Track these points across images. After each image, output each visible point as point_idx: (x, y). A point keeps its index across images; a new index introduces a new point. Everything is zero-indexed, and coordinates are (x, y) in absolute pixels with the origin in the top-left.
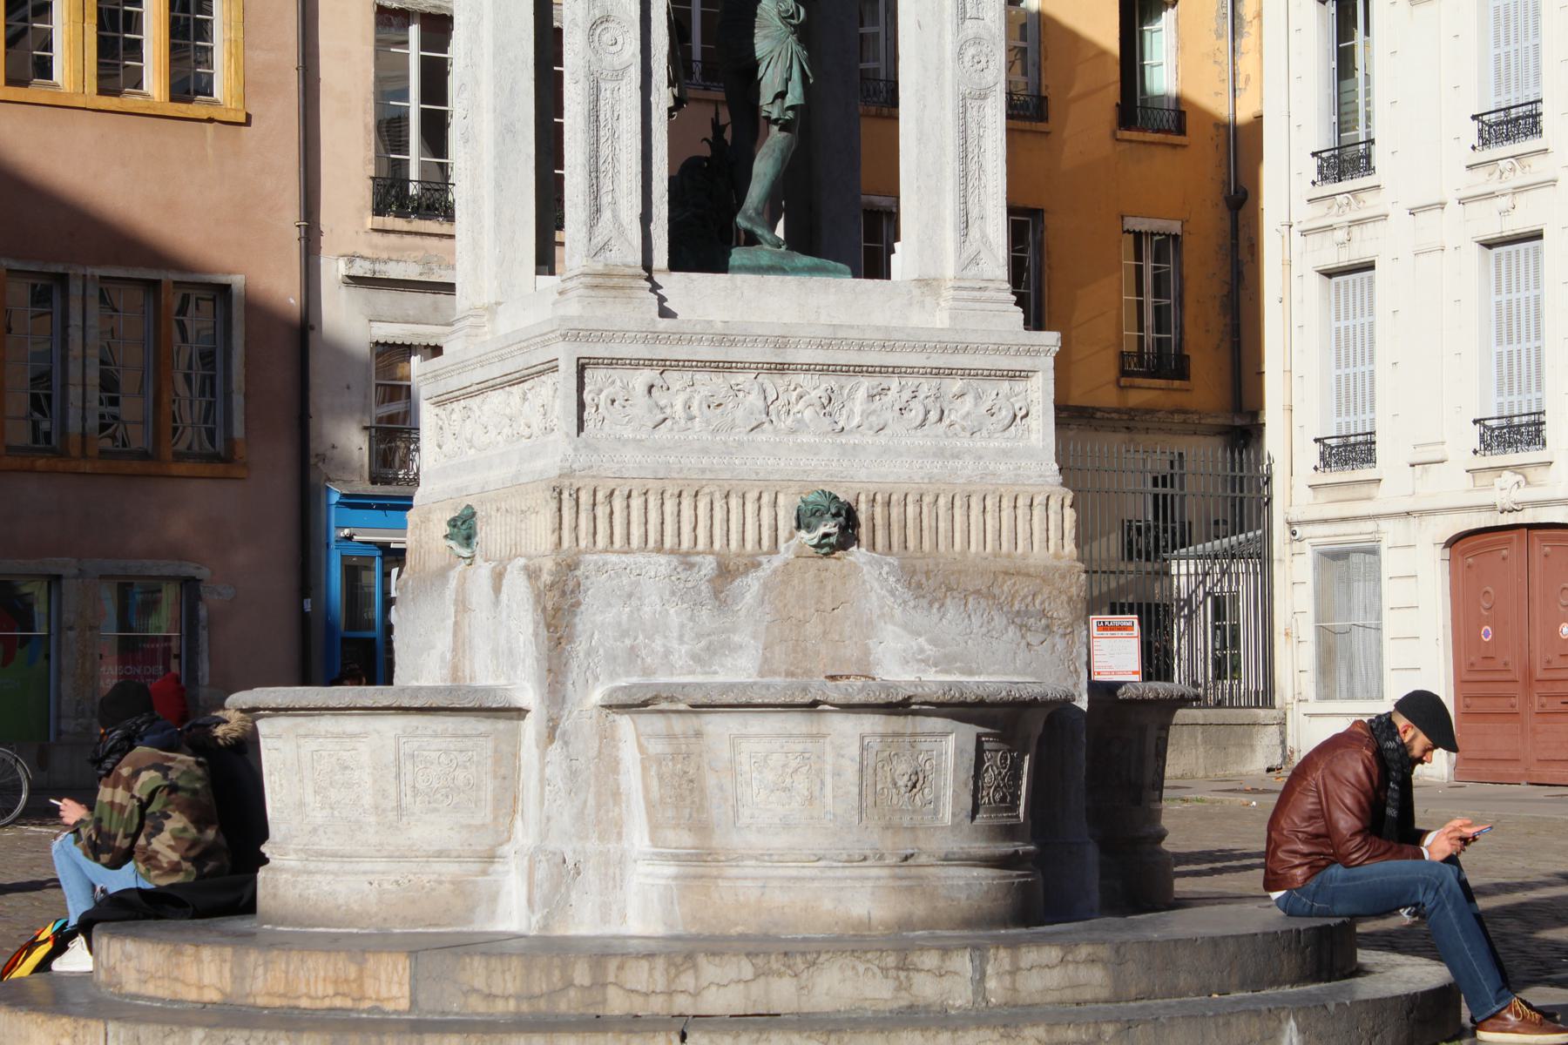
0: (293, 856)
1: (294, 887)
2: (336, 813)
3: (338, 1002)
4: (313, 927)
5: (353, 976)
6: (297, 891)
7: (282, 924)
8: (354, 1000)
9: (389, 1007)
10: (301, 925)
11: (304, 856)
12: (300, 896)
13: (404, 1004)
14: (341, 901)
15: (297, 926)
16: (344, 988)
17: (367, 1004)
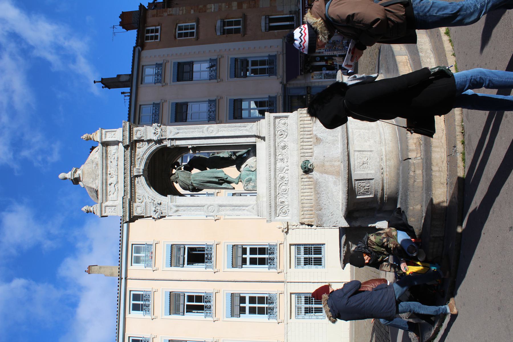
0: (382, 147)
1: (389, 144)
2: (371, 137)
3: (409, 65)
4: (397, 137)
5: (403, 63)
6: (390, 143)
7: (398, 148)
8: (408, 63)
9: (407, 58)
10: (398, 140)
11: (382, 144)
12: (391, 142)
13: (406, 56)
14: (390, 131)
15: (398, 142)
16: (406, 64)
17: (408, 61)
